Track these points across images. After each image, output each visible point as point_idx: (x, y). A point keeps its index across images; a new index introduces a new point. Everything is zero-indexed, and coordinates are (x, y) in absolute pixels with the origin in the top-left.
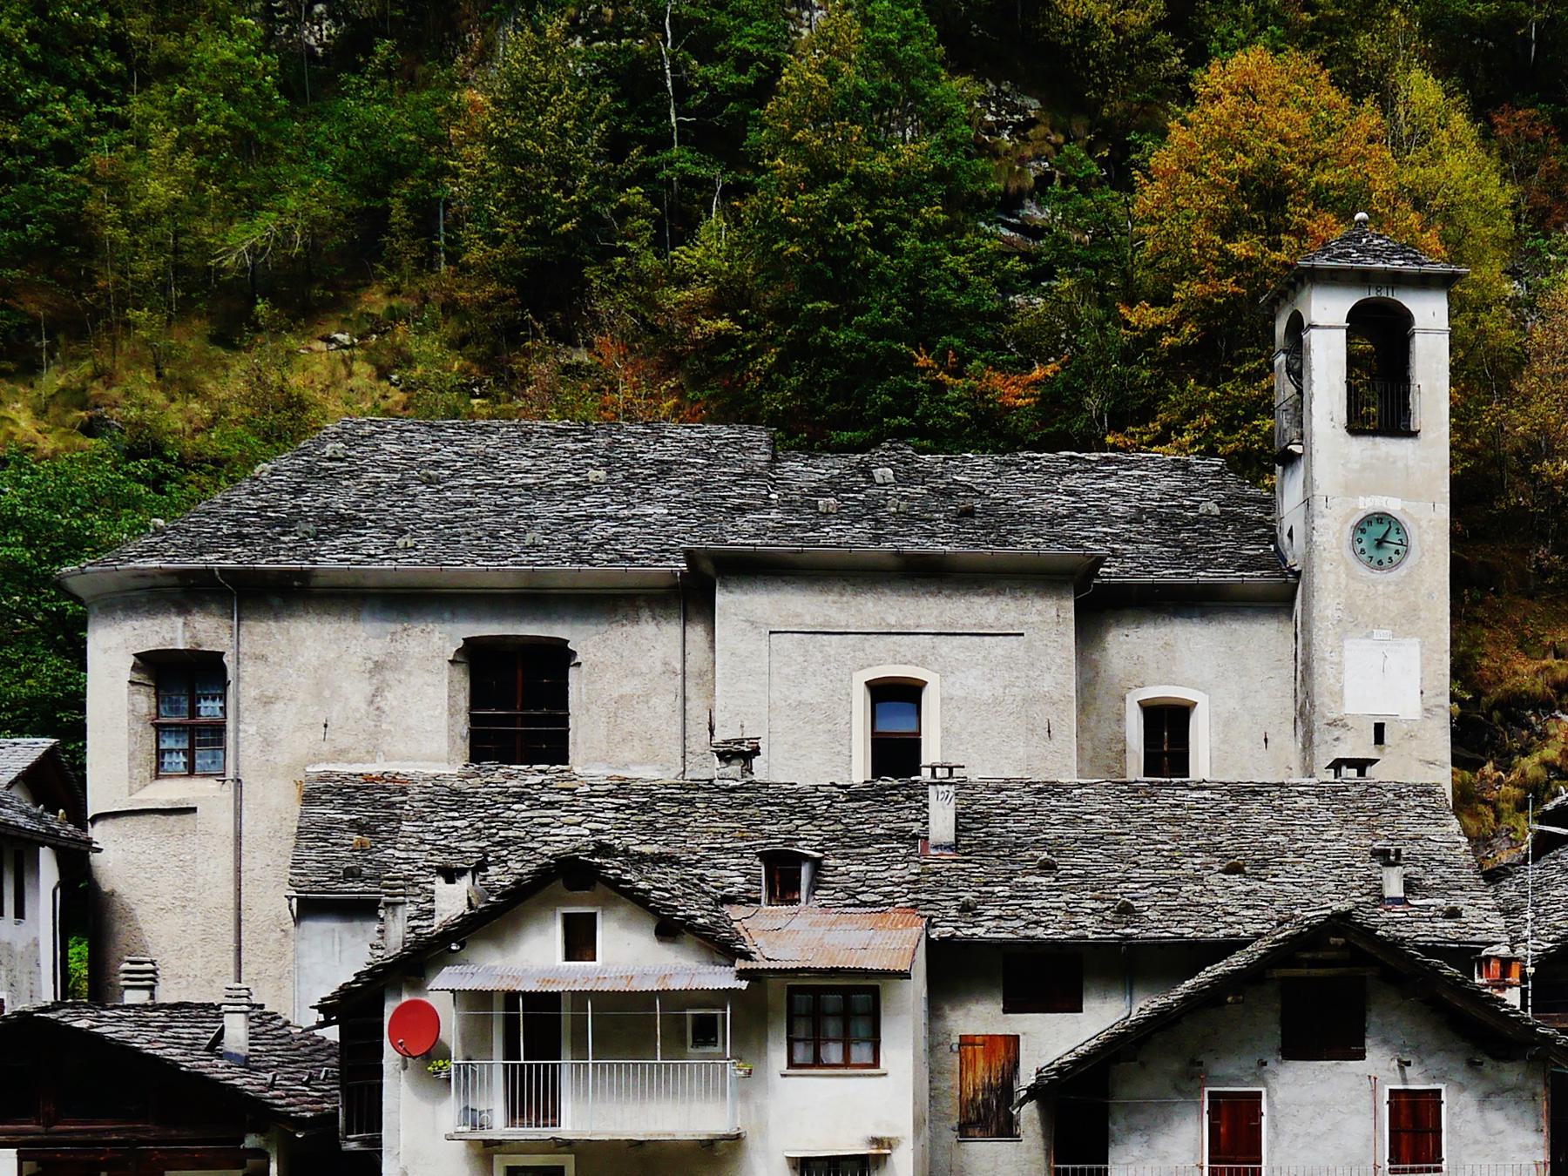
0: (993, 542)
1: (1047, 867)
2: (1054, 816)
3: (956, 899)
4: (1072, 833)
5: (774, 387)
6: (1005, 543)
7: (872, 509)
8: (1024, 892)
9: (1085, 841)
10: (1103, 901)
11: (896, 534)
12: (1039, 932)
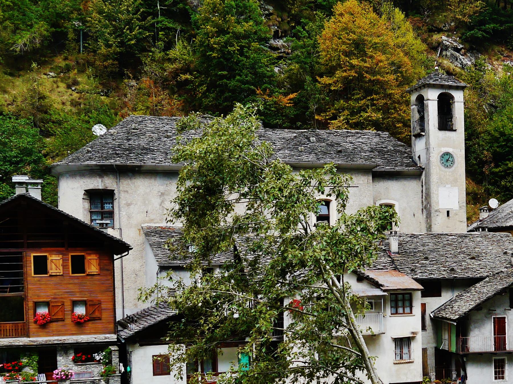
0: (350, 161)
1: (426, 259)
2: (418, 244)
3: (408, 267)
4: (426, 248)
5: (207, 97)
6: (354, 161)
7: (312, 151)
8: (425, 266)
9: (431, 251)
10: (445, 267)
11: (323, 158)
12: (432, 276)
